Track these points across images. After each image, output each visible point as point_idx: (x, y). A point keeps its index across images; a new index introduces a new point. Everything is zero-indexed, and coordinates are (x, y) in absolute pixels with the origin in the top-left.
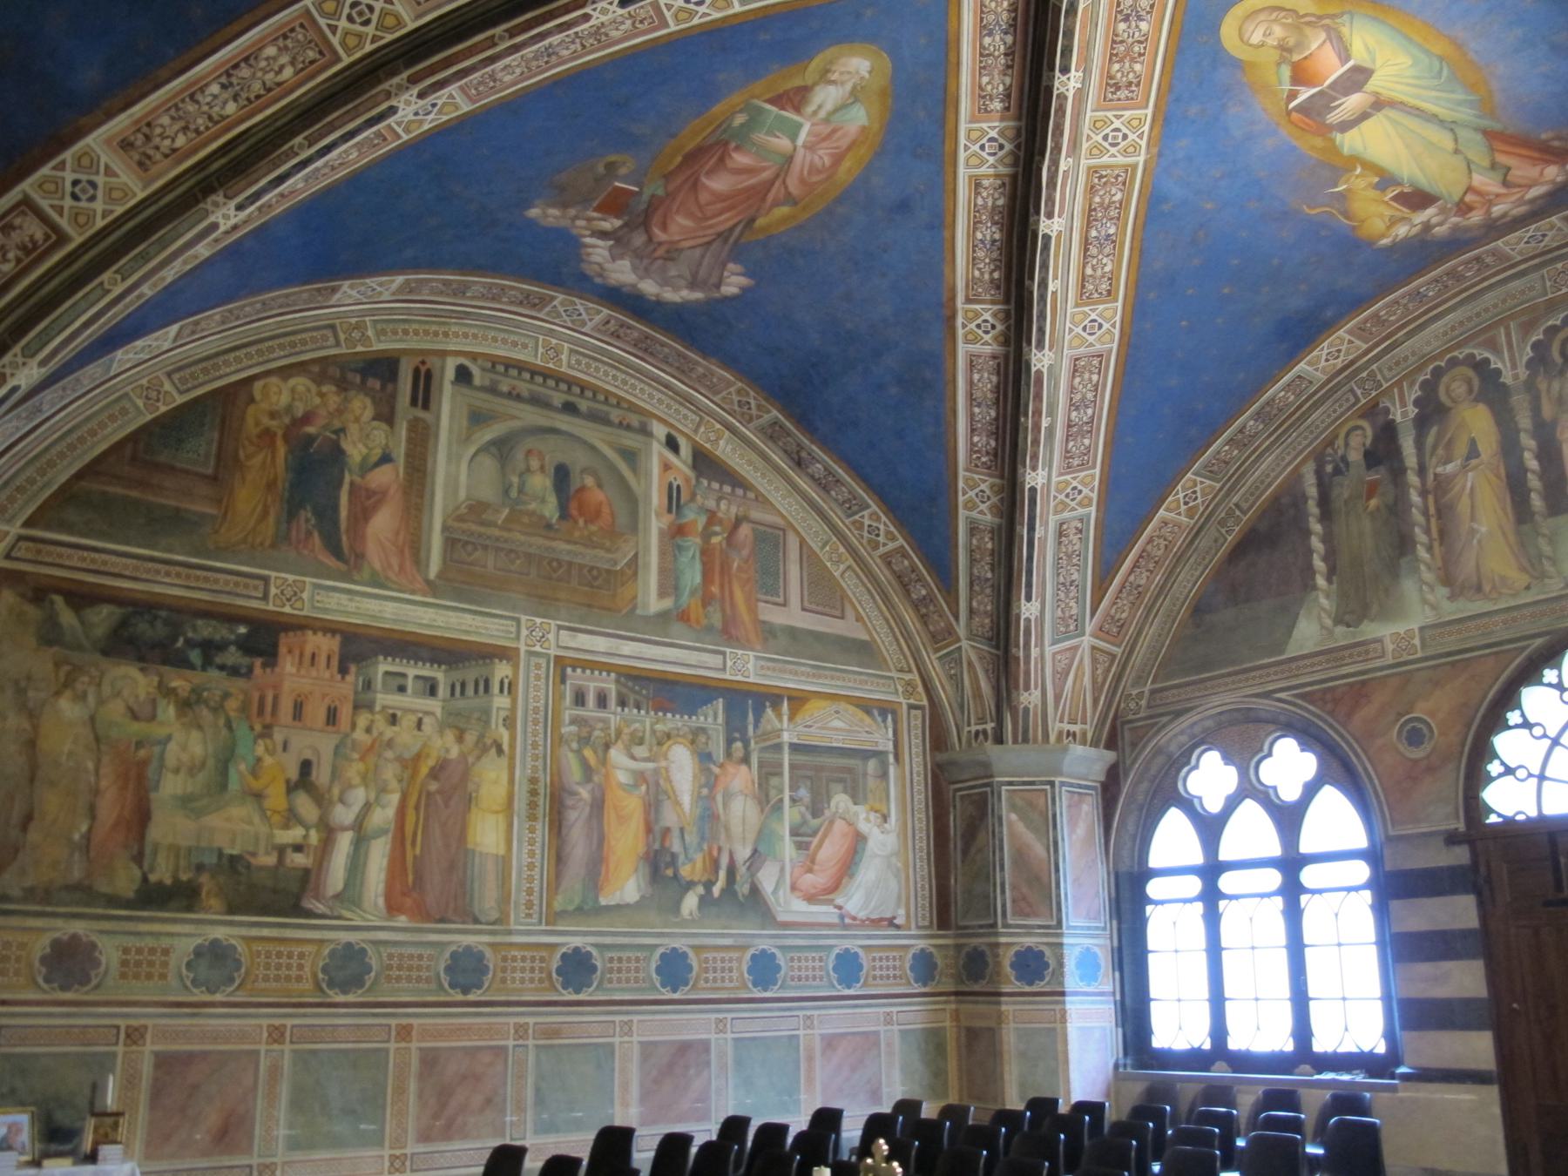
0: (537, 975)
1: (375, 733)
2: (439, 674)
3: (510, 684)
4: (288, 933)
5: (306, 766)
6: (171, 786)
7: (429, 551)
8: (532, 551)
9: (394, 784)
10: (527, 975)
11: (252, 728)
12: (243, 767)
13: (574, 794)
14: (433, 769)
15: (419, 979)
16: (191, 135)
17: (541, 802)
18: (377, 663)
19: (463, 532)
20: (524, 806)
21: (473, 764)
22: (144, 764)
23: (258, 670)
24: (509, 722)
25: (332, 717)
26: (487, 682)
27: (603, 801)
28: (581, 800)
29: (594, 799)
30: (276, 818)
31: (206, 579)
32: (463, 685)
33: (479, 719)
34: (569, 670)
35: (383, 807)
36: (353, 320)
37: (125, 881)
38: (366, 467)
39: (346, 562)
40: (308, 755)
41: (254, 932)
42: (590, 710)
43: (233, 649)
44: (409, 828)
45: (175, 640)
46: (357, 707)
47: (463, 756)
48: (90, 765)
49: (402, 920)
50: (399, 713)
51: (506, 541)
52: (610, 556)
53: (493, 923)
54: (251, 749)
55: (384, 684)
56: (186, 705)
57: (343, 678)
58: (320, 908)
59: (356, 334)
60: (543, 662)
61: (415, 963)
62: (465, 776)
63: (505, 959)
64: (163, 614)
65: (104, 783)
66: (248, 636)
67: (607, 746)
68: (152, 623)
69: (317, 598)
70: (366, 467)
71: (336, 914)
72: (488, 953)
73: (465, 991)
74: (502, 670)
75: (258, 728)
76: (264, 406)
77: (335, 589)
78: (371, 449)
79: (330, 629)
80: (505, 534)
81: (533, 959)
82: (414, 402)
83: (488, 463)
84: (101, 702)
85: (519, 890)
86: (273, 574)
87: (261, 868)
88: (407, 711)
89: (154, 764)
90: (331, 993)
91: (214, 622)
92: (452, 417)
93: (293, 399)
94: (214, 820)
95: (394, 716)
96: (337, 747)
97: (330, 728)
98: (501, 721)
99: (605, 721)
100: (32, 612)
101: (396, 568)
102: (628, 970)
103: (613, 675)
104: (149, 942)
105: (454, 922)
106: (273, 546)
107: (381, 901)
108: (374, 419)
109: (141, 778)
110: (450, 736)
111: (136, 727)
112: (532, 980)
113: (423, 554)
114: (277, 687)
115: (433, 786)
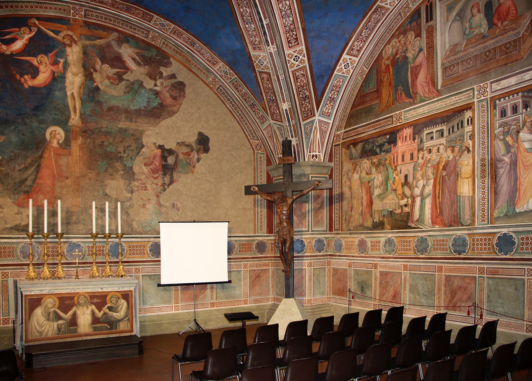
0: (487, 247)
1: (425, 158)
2: (444, 127)
3: (471, 119)
4: (405, 235)
5: (406, 176)
6: (377, 192)
7: (437, 78)
8: (476, 53)
9: (431, 176)
10: (483, 247)
11: (392, 169)
12: (391, 182)
13: (501, 161)
14: (444, 166)
15: (443, 249)
16: (257, 37)
17: (487, 169)
18: (424, 131)
19: (449, 62)
20: (479, 172)
21: (458, 160)
22: (370, 187)
23: (392, 149)
24: (472, 137)
25: (412, 158)
26: (462, 122)
27: (516, 161)
28: (506, 162)
29: (511, 161)
30: (400, 197)
31: (379, 124)
32: (453, 128)
33: (460, 140)
34: (497, 101)
35: (429, 186)
36: (405, 6)
37: (369, 223)
38: (415, 59)
39: (412, 98)
40: (406, 173)
41: (398, 235)
42: (510, 117)
43: (386, 144)
44: (437, 192)
45: (374, 148)
46: (418, 151)
47: (454, 157)
48: (361, 191)
49: (437, 227)
50: (431, 148)
51: (466, 55)
52: (516, 31)
53: (469, 225)
54: (392, 175)
55: (426, 138)
56: (377, 166)
57: (414, 142)
58: (413, 225)
59: (407, 10)
60: (485, 103)
61: (442, 243)
62: (455, 167)
63: (474, 240)
64: (371, 140)
65: (363, 195)
66: (389, 138)
67: (518, 132)
68: (368, 144)
69: (406, 116)
70: (415, 59)
71: (417, 227)
72: (467, 238)
73: (459, 254)
74: (468, 114)
75: (393, 168)
76: (386, 57)
77: (410, 110)
78: (415, 50)
79: (408, 125)
80: (465, 53)
81: (485, 240)
82: (427, 21)
83: (456, 25)
84: (361, 172)
85: (479, 210)
86: (394, 114)
87: (398, 214)
88: (434, 146)
89: (372, 187)
90: (418, 254)
91: (381, 138)
92: (441, 16)
93: (392, 49)
94: (386, 201)
95: (430, 149)
96: (414, 167)
97: (412, 161)
98: (468, 138)
99: (517, 120)
100: (348, 152)
101: (427, 91)
102: (481, 244)
103: (520, 94)
104: (376, 239)
105: (454, 226)
106: (393, 104)
107: (430, 220)
108: (415, 38)
109: (370, 192)
110: (449, 151)
111: (368, 176)
112: (485, 249)
113: (436, 81)
114: (397, 152)
115: (444, 173)
